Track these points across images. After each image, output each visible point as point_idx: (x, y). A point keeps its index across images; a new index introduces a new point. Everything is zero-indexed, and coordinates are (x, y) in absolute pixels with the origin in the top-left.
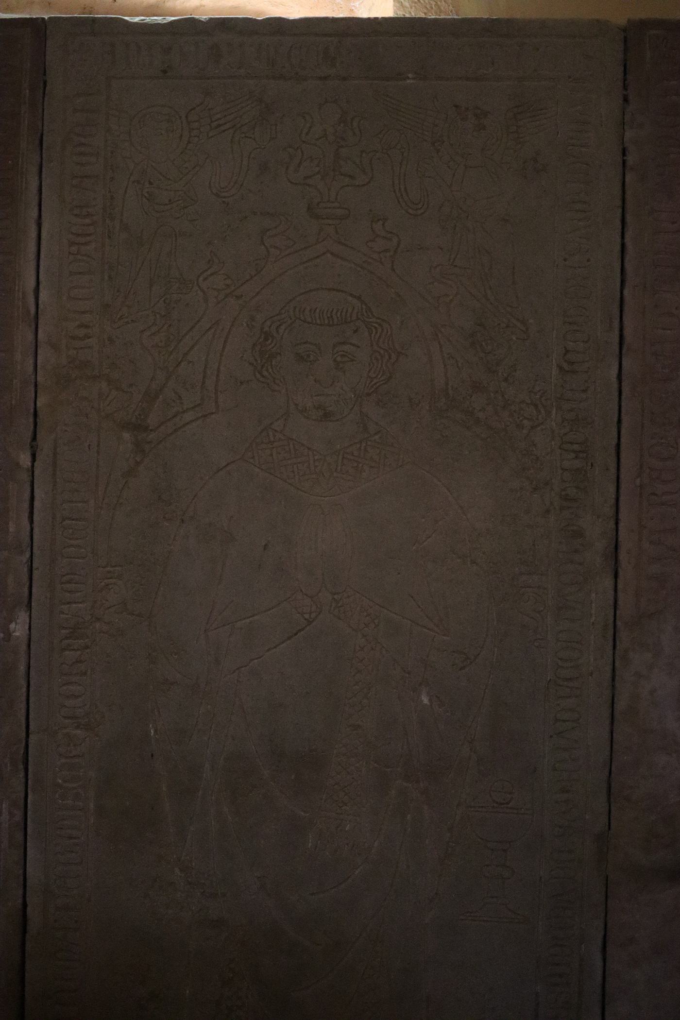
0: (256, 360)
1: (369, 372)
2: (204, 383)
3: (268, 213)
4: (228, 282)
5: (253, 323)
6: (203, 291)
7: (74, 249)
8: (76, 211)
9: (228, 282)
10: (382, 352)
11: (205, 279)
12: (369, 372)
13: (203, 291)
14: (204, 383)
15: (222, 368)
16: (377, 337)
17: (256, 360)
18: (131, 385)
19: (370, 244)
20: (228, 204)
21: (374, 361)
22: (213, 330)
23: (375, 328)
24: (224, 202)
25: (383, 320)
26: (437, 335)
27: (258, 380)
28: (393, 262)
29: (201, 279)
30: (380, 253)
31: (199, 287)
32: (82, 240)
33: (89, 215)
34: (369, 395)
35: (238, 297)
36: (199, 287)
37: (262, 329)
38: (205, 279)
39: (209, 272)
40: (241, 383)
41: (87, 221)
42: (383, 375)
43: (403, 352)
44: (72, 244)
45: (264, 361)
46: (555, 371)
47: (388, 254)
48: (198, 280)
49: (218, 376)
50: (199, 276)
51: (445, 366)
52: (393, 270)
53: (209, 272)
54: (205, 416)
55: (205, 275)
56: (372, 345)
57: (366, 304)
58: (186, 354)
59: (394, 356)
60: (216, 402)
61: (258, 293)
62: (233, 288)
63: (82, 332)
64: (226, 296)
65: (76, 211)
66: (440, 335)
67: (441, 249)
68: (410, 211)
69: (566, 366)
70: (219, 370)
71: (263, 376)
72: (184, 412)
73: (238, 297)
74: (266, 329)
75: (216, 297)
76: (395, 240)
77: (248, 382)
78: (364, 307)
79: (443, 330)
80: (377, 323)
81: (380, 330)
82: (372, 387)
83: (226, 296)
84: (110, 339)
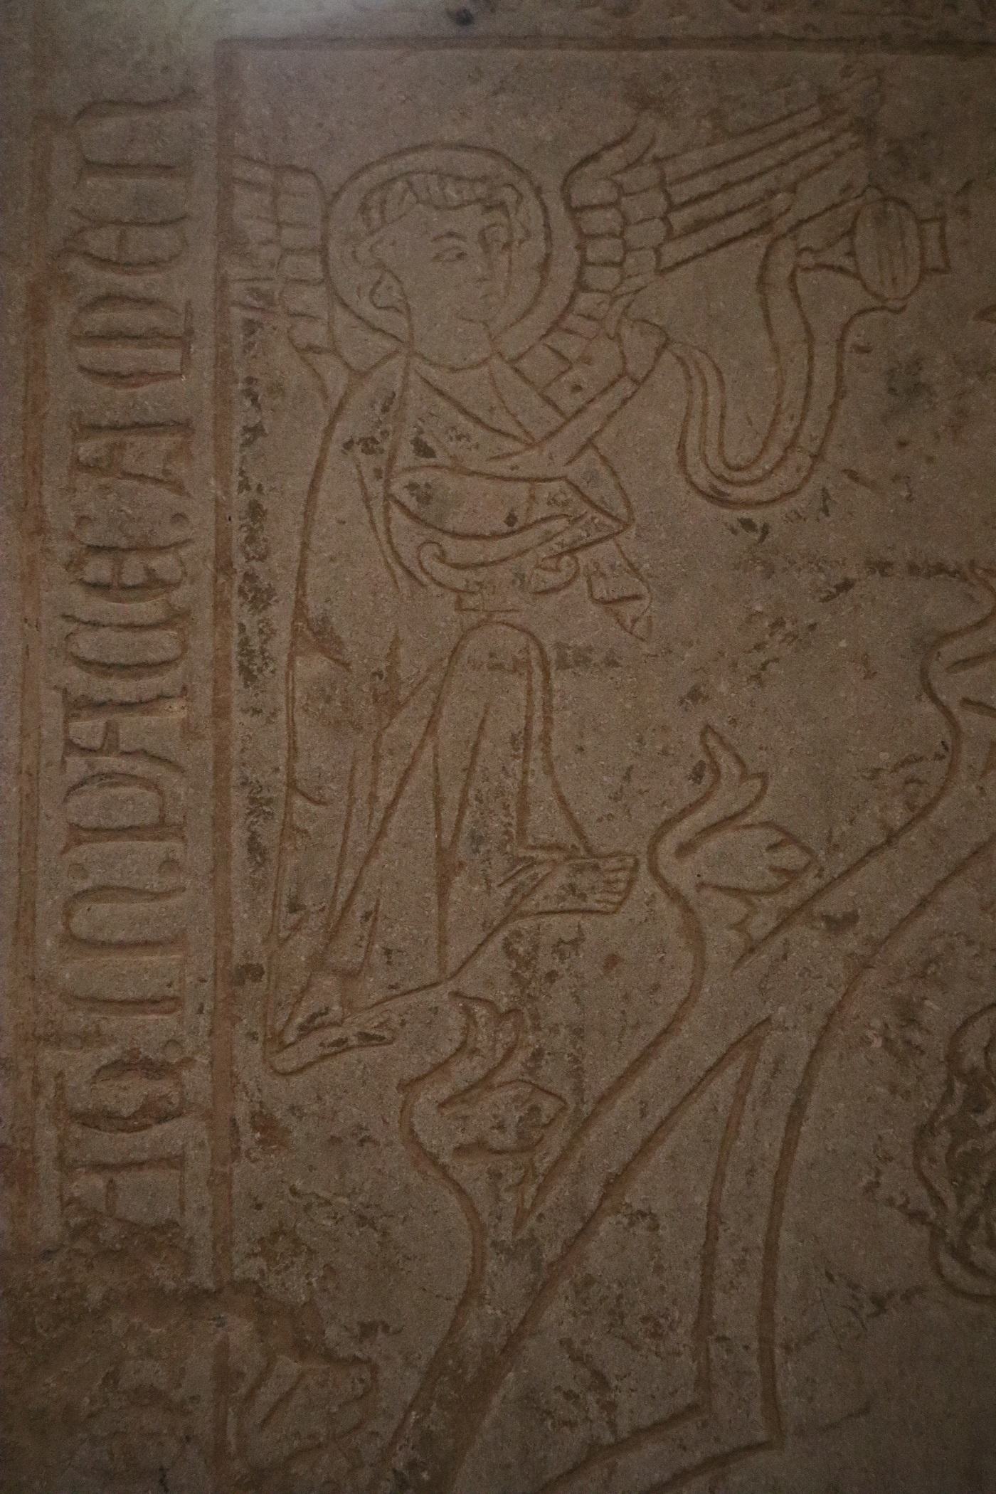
0: (938, 1200)
2: (705, 1303)
3: (941, 569)
4: (790, 857)
5: (917, 1037)
6: (675, 896)
7: (88, 728)
8: (99, 569)
9: (790, 857)
11: (684, 849)
13: (675, 896)
14: (705, 1303)
15: (786, 1238)
17: (938, 1200)
18: (367, 1330)
20: (765, 530)
22: (732, 1072)
24: (748, 524)
27: (952, 1288)
29: (668, 845)
31: (664, 884)
32: (123, 689)
33: (153, 584)
35: (838, 925)
36: (664, 884)
37: (953, 1058)
38: (684, 849)
39: (700, 818)
40: (880, 1303)
41: (147, 609)
44: (76, 706)
45: (973, 1200)
48: (653, 850)
49: (769, 1275)
50: (658, 837)
53: (700, 818)
54: (720, 1461)
55: (684, 830)
58: (614, 1184)
60: (770, 1397)
61: (923, 903)
62: (811, 882)
63: (130, 1093)
64: (786, 919)
65: (99, 569)
70: (771, 1248)
71: (971, 1267)
72: (620, 1446)
73: (838, 925)
74: (973, 1058)
75: (740, 926)
77: (907, 1297)
83: (786, 919)
84: (265, 1124)
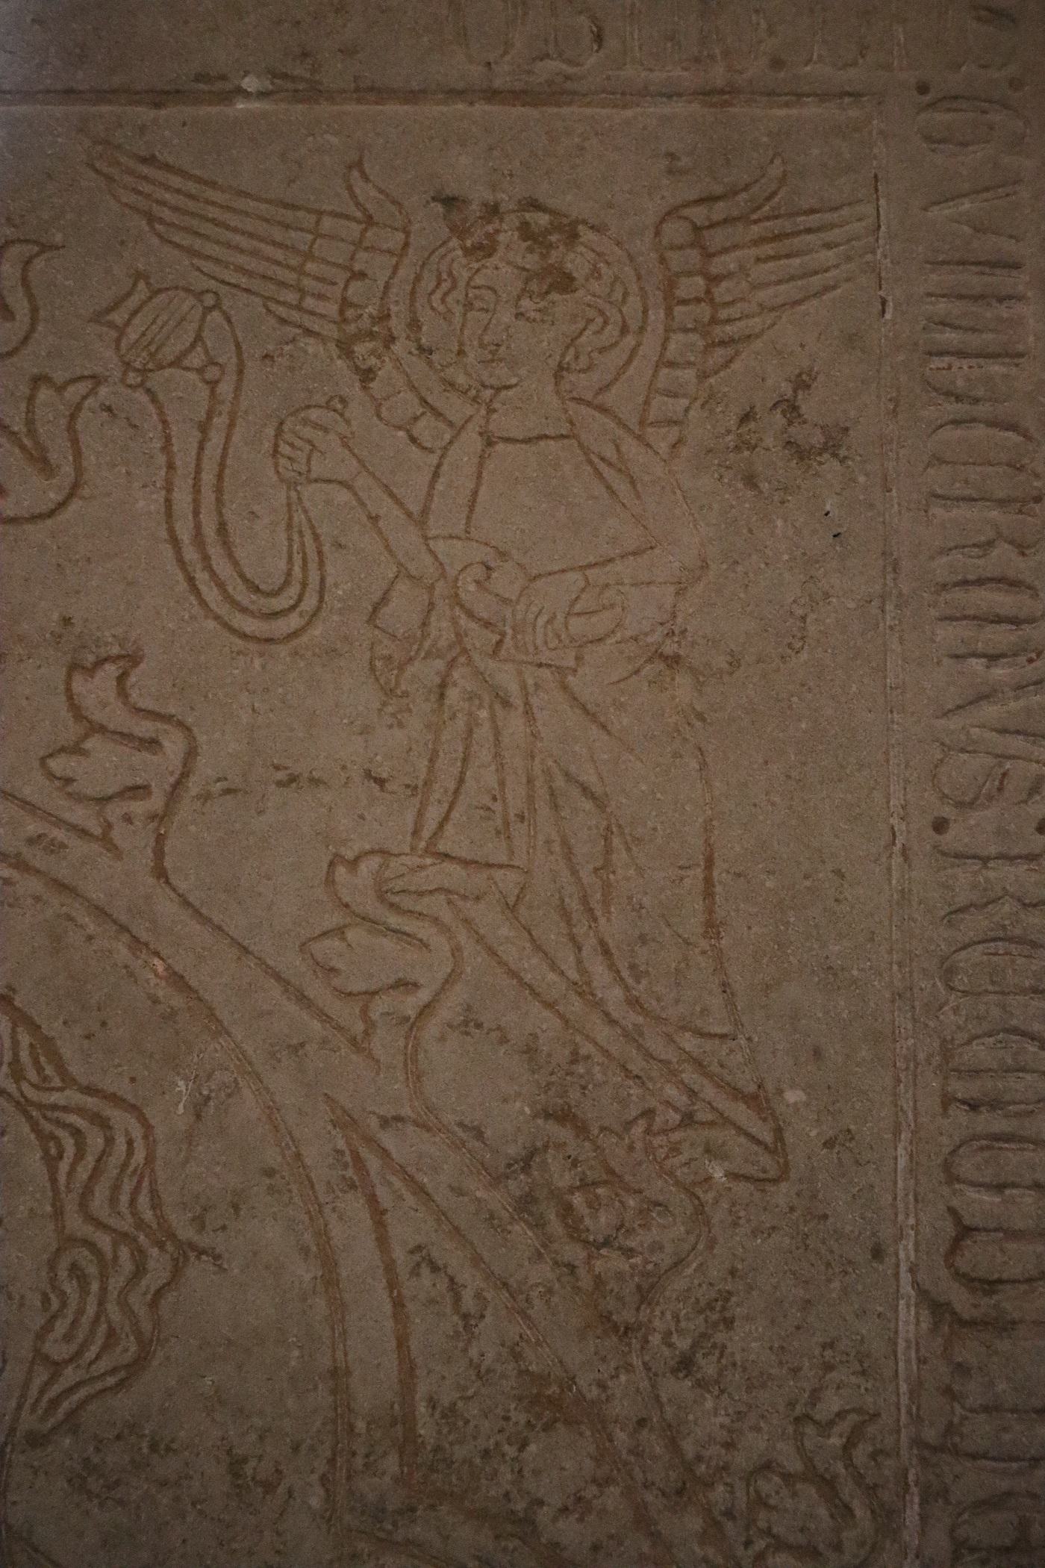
1: (40, 1336)
10: (104, 1241)
12: (40, 1336)
16: (83, 1173)
19: (56, 765)
21: (70, 1288)
23: (76, 1133)
25: (115, 1099)
26: (358, 1161)
28: (160, 839)
30: (104, 800)
34: (36, 1440)
42: (106, 1347)
43: (204, 1241)
46: (909, 1321)
47: (138, 807)
51: (398, 1304)
52: (161, 873)
56: (58, 1213)
57: (34, 1028)
59: (159, 1265)
66: (373, 1163)
67: (381, 782)
68: (250, 625)
69: (961, 1300)
76: (174, 745)
78: (25, 1039)
79: (387, 1139)
80: (80, 1111)
81: (96, 1141)
82: (55, 1403)
